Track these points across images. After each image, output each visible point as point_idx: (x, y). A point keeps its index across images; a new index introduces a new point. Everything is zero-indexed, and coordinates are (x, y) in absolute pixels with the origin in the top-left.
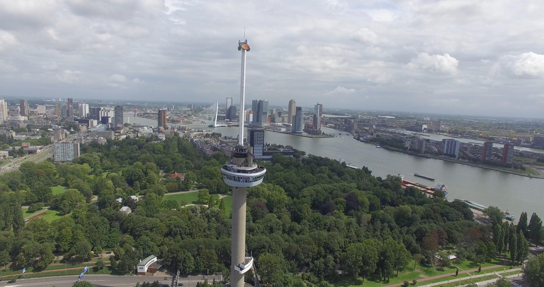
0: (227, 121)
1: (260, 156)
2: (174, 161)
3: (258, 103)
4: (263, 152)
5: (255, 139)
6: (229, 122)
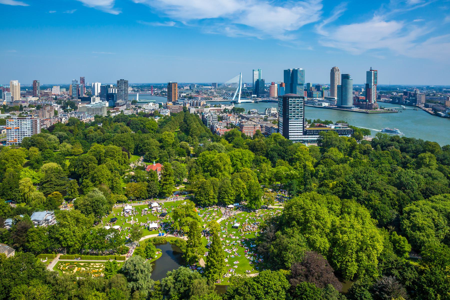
0: (254, 97)
1: (300, 136)
2: (161, 144)
3: (291, 71)
4: (303, 130)
5: (291, 110)
6: (256, 98)
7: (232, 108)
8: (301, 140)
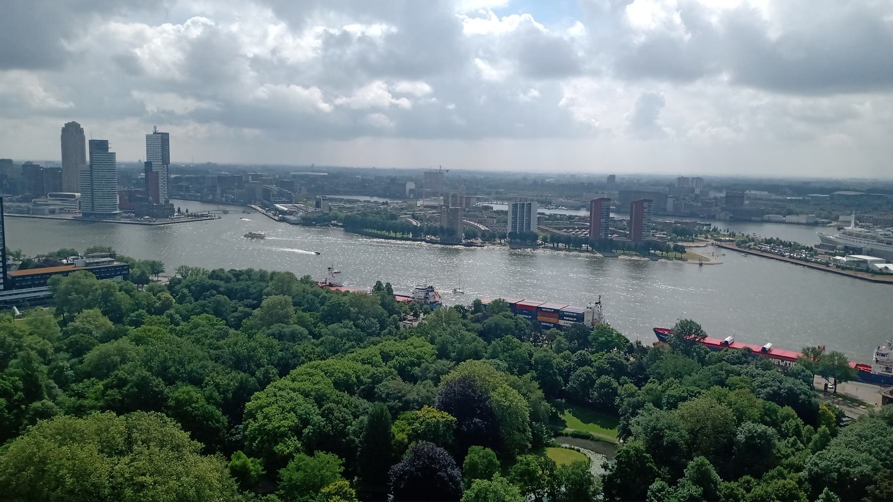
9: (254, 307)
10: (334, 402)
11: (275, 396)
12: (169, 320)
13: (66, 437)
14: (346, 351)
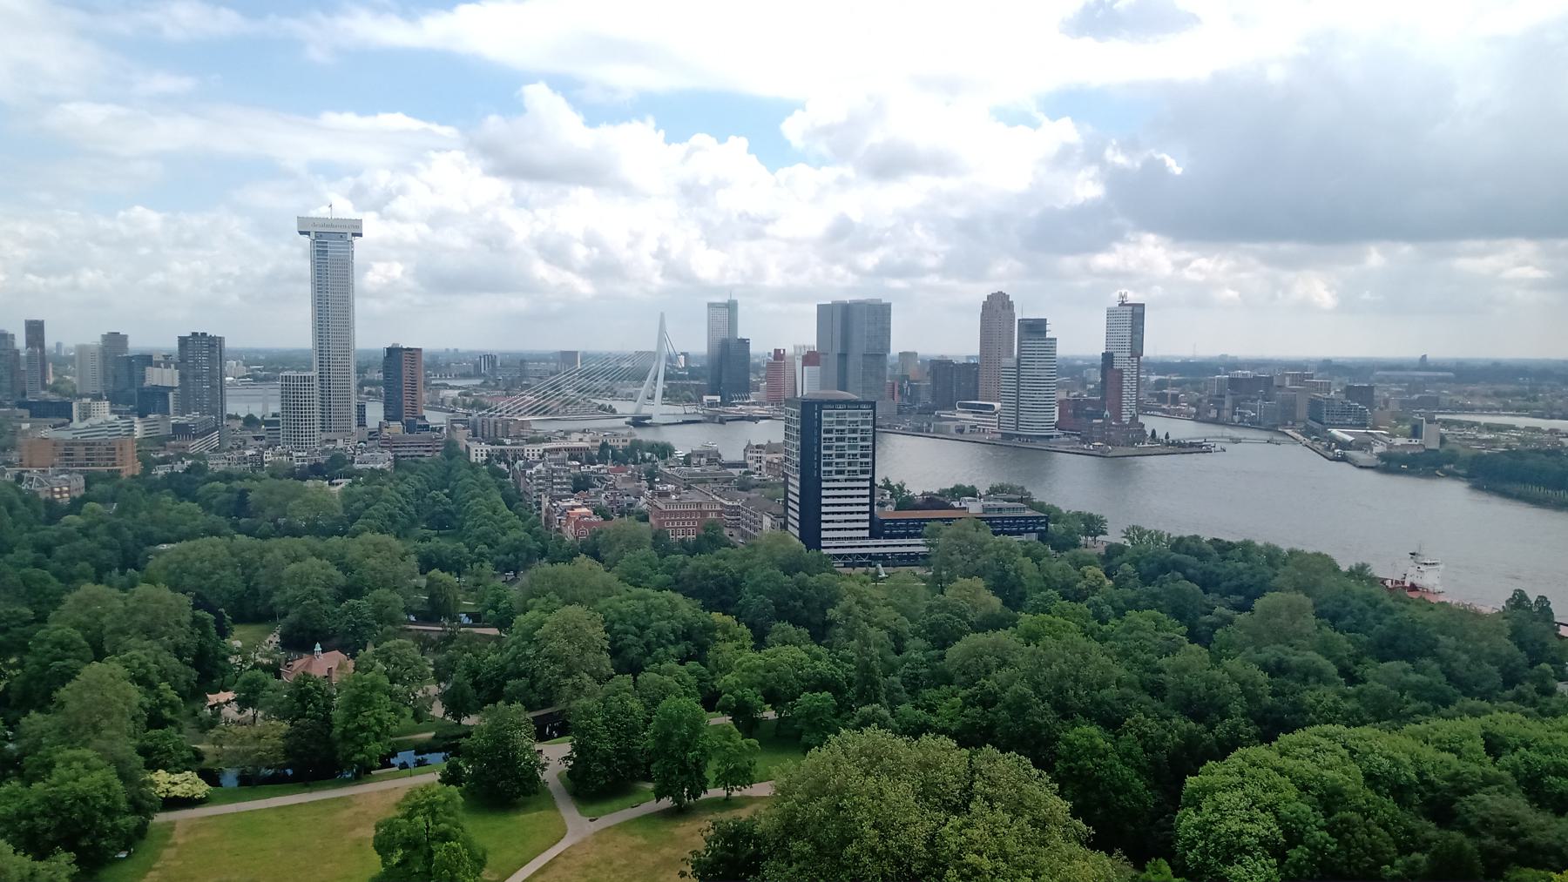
0: (712, 404)
1: (859, 543)
4: (871, 520)
7: (627, 444)
8: (864, 555)
9: (1240, 608)
10: (1358, 809)
11: (1242, 774)
12: (1090, 612)
13: (873, 762)
14: (1408, 717)
